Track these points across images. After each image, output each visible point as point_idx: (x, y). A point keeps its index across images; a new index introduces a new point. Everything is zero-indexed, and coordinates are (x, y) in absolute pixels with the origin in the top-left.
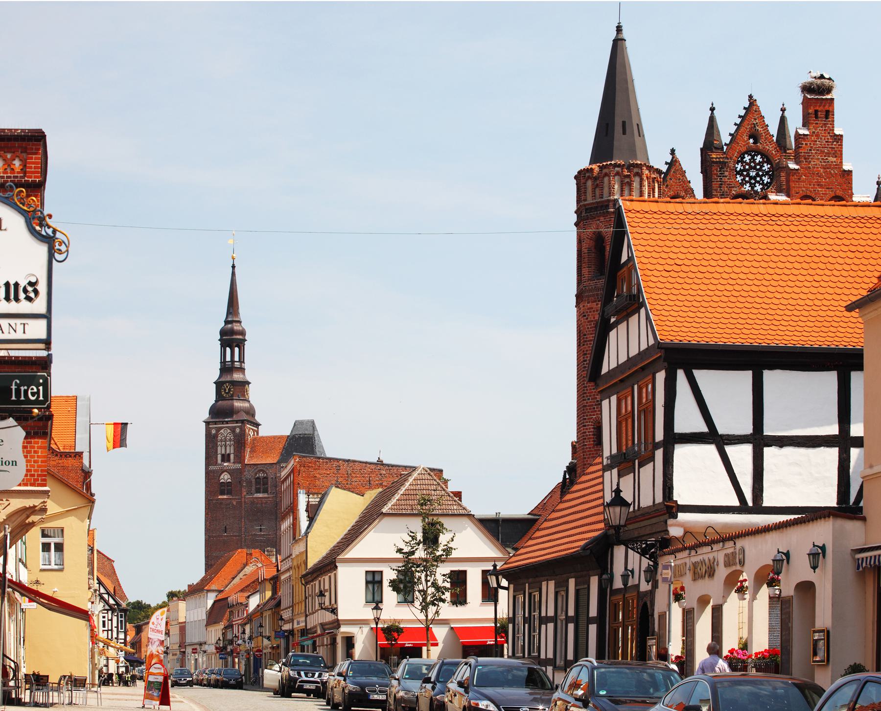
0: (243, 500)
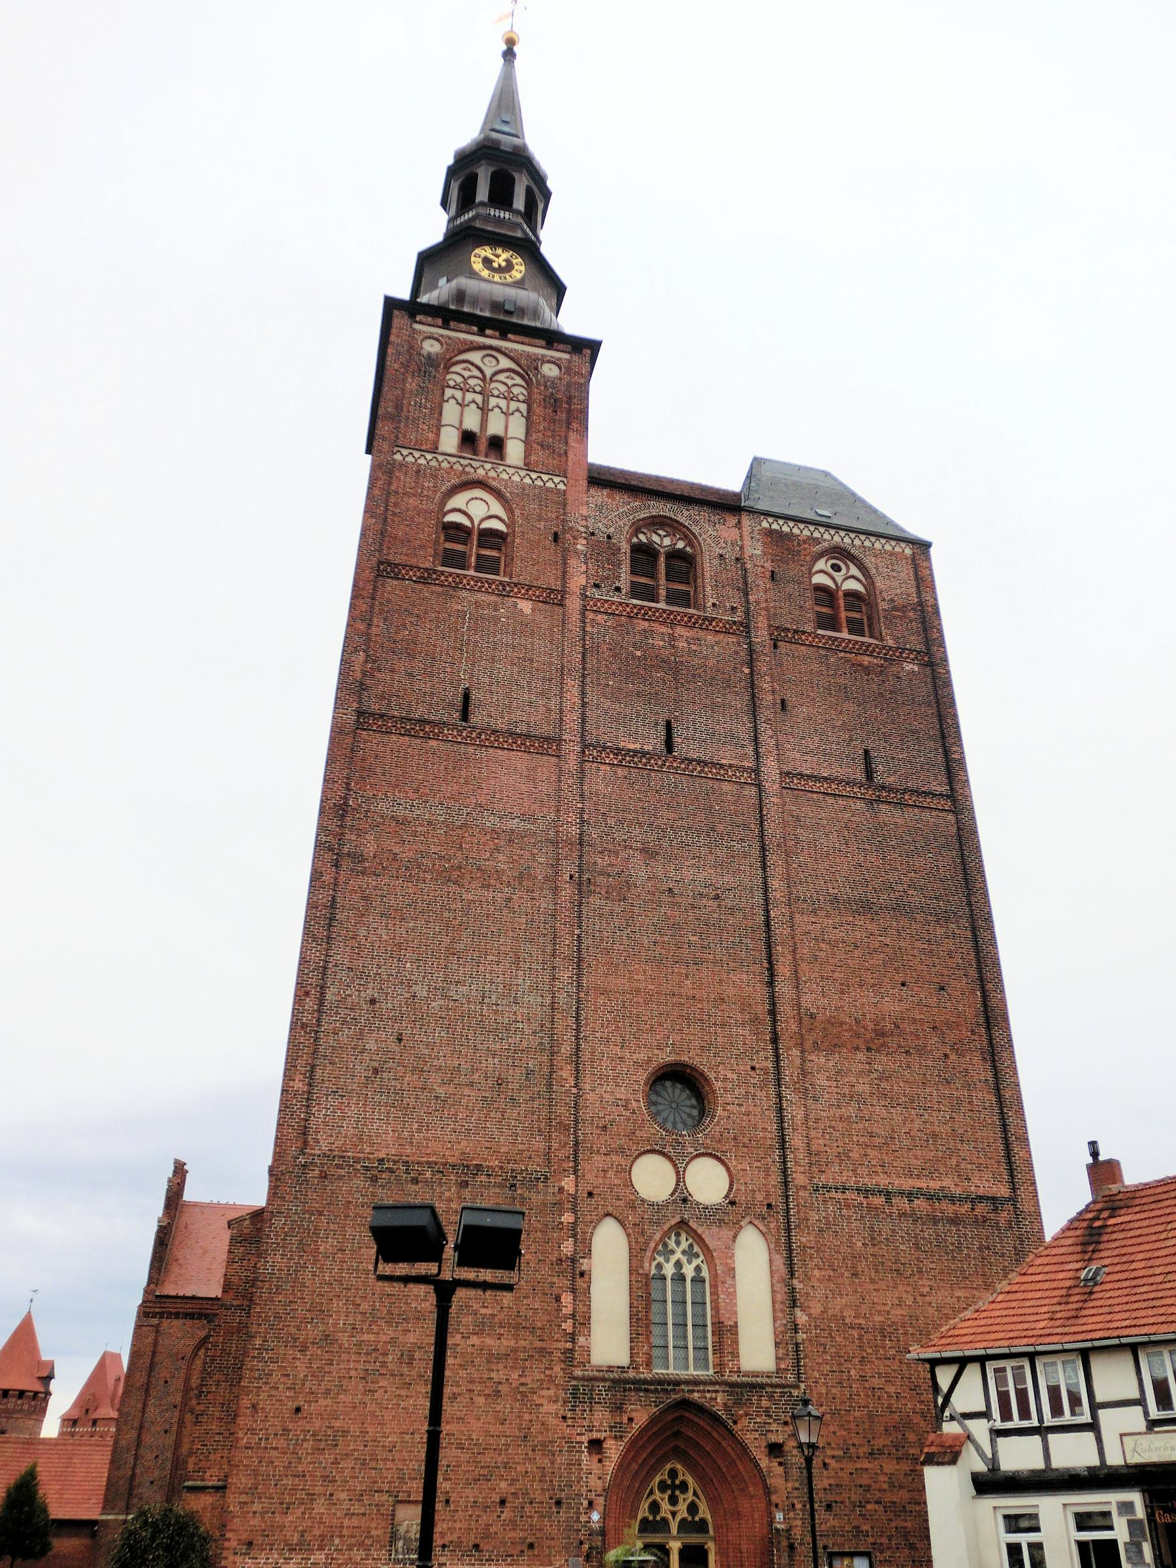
0: (574, 604)
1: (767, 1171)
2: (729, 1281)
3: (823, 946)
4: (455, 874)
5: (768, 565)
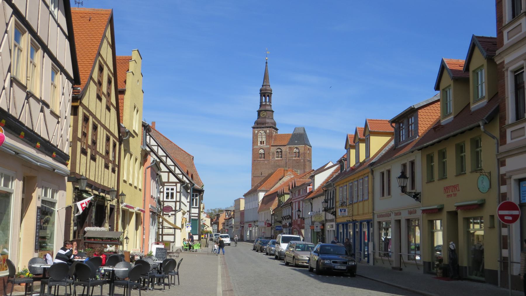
5: (289, 151)
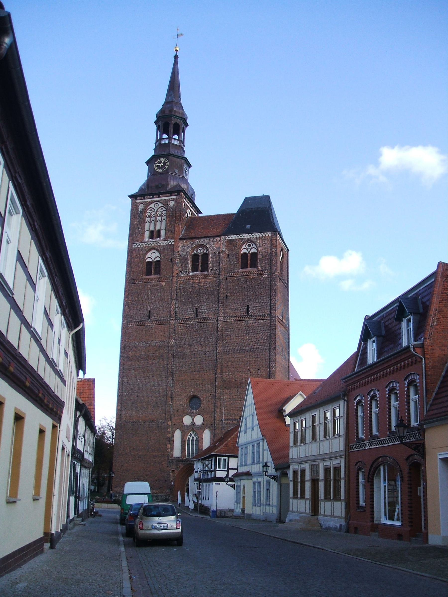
0: (175, 280)
1: (211, 418)
2: (201, 441)
3: (230, 363)
4: (147, 358)
